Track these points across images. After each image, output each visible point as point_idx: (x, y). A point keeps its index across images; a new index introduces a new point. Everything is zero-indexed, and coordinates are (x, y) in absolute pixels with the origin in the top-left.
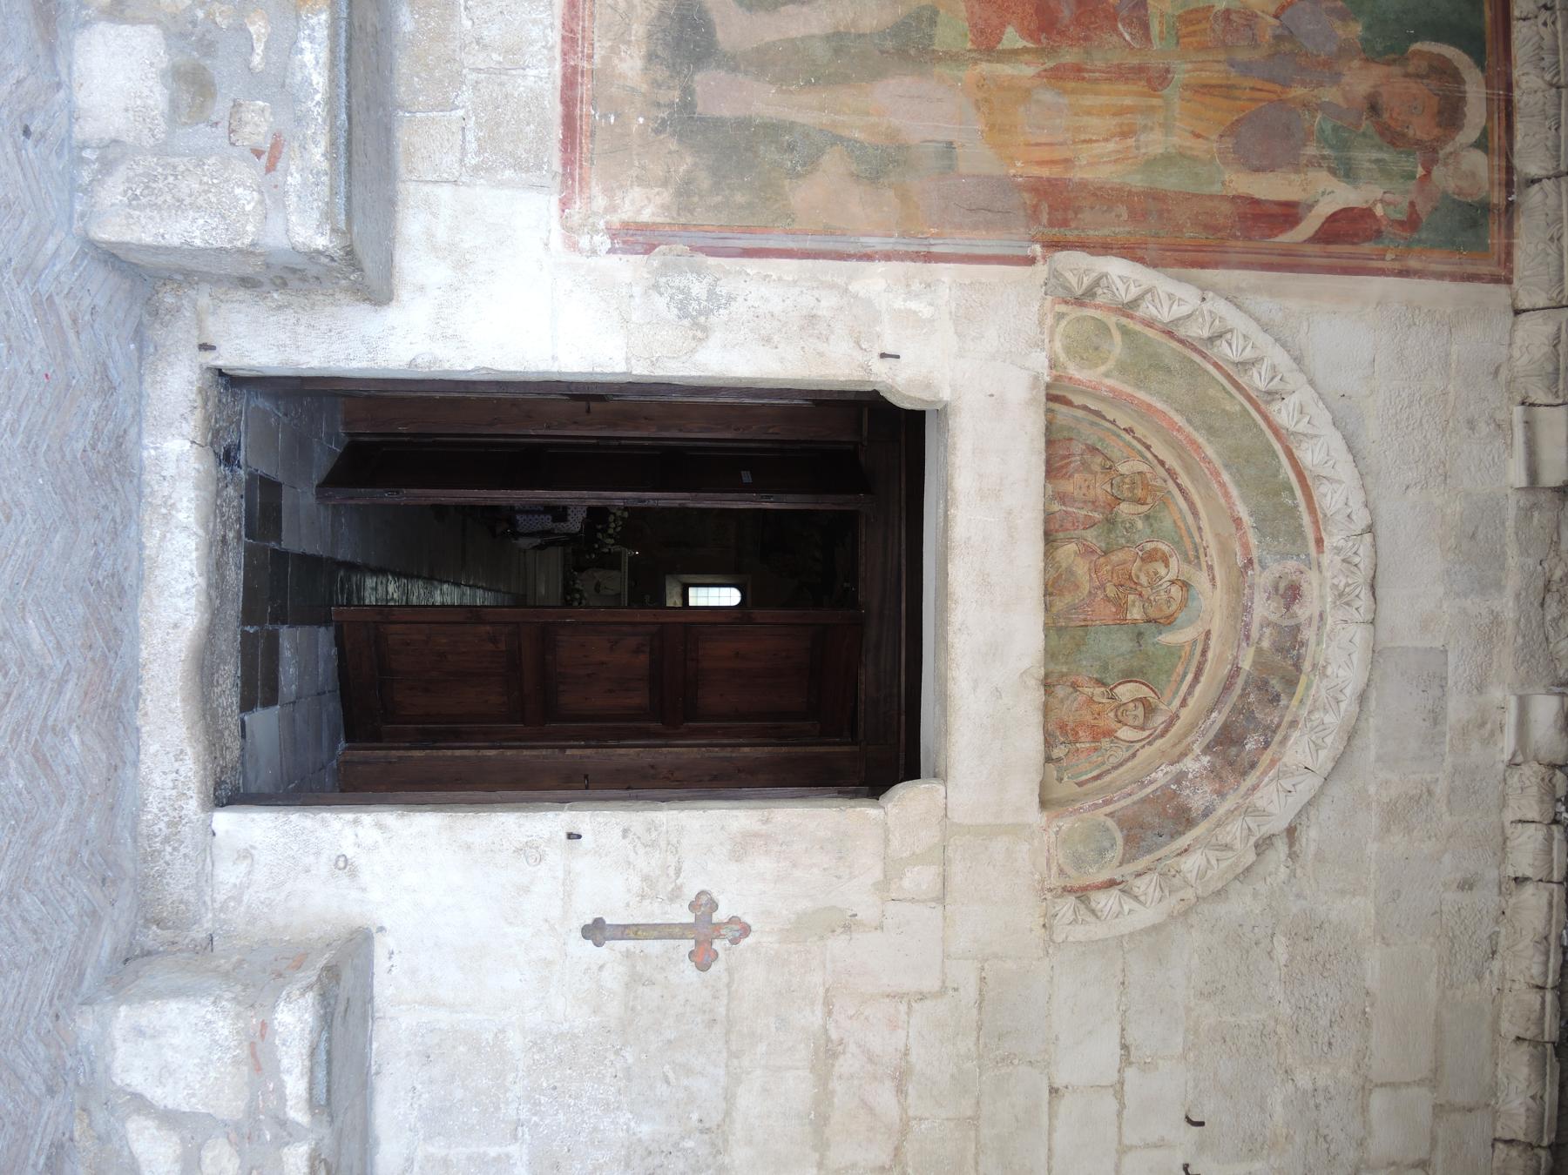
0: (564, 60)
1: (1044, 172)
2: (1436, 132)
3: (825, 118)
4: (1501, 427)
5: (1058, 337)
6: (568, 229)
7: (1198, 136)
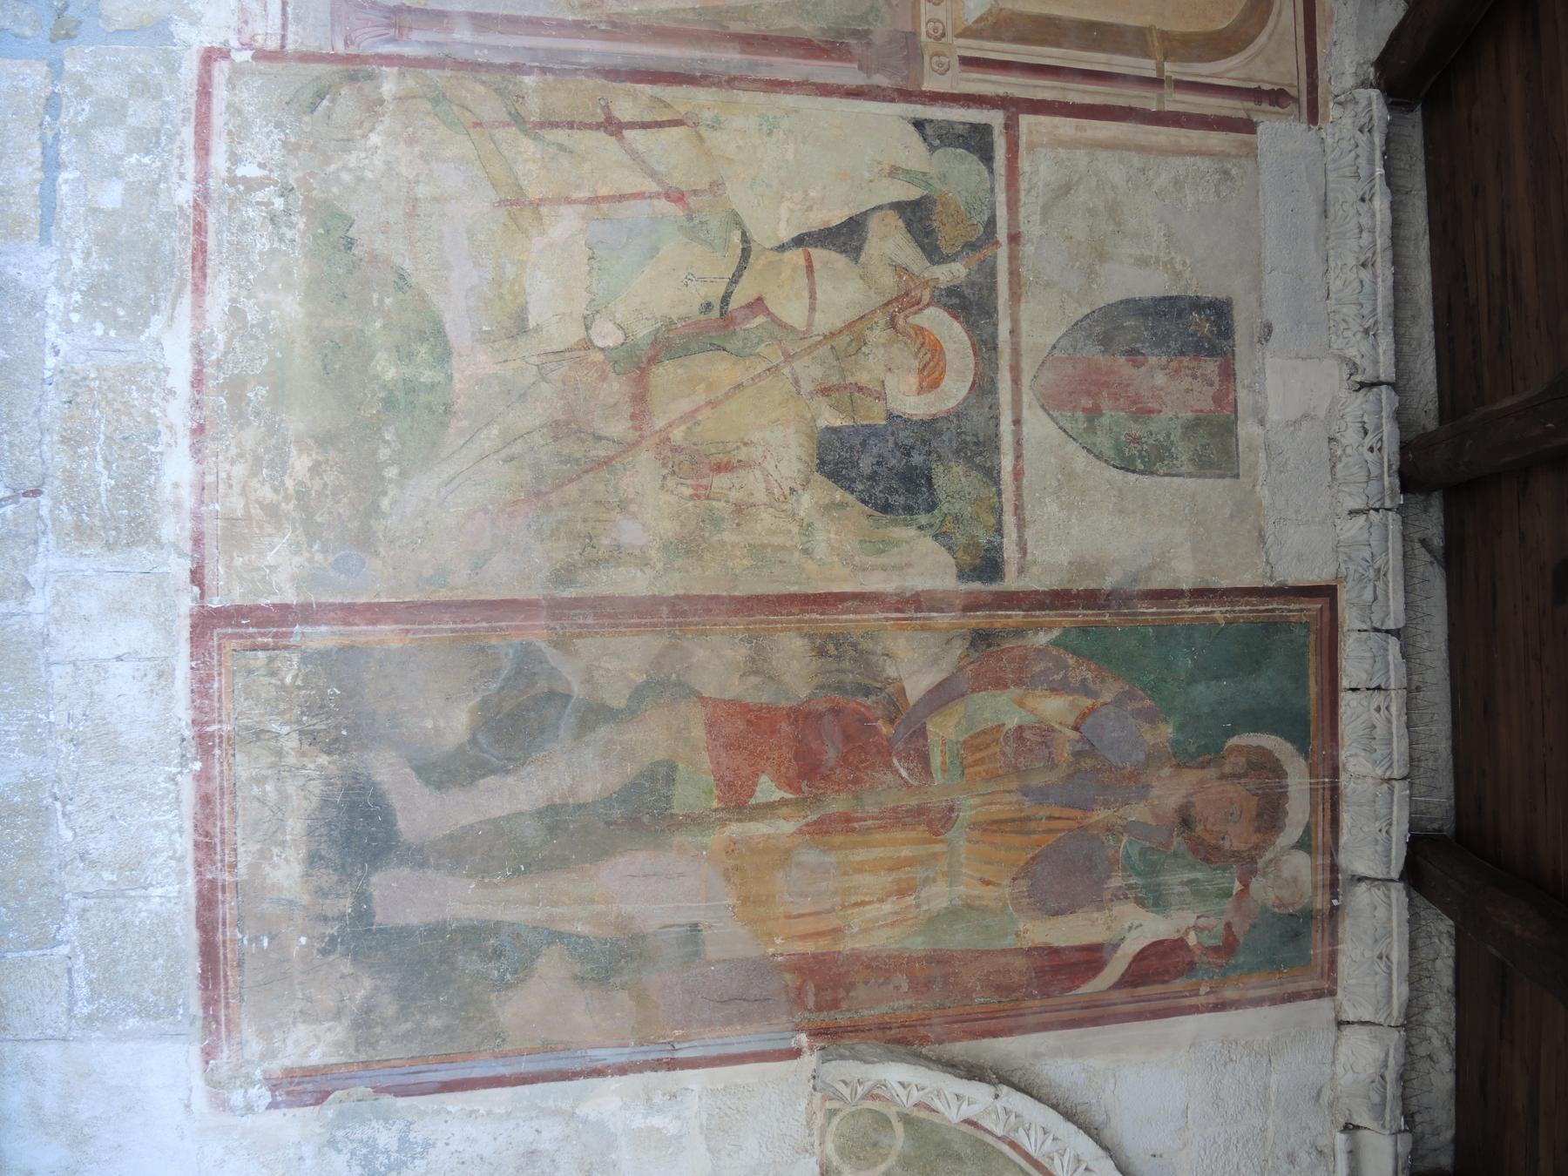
0: (199, 873)
1: (809, 947)
2: (1254, 838)
3: (539, 913)
5: (829, 1138)
6: (213, 1083)
7: (987, 883)
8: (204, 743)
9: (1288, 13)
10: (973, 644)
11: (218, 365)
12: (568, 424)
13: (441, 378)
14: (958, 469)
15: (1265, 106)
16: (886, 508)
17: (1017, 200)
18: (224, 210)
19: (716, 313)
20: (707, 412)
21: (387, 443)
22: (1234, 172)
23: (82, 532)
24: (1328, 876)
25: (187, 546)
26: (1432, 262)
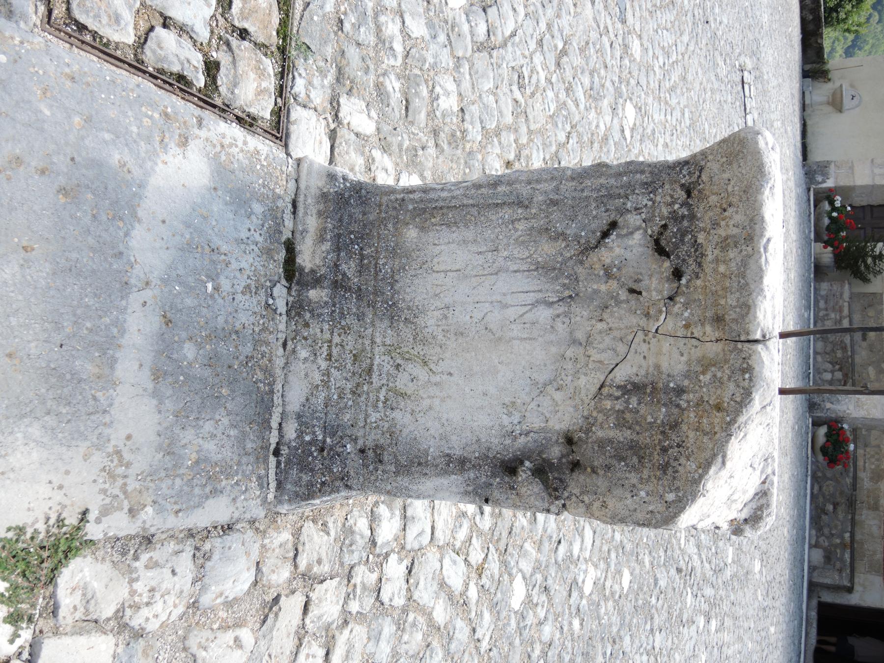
23: (869, 509)
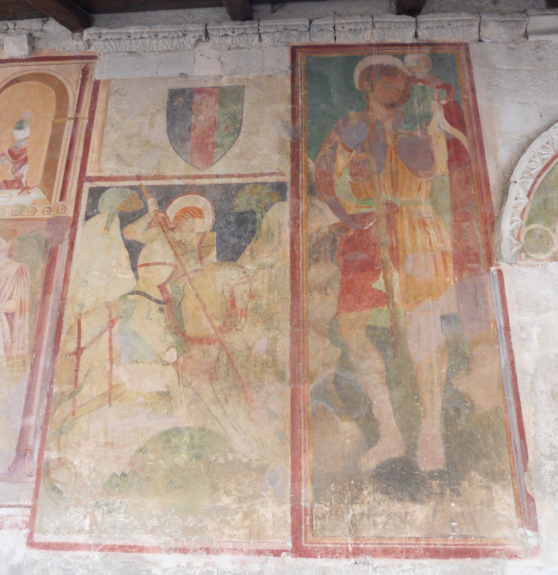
0: (421, 557)
1: (451, 266)
2: (399, 77)
3: (437, 390)
4: (538, 46)
7: (420, 188)
8: (357, 552)
9: (50, 67)
10: (314, 195)
11: (177, 540)
12: (211, 373)
13: (187, 432)
14: (237, 201)
15: (89, 76)
16: (253, 232)
17: (122, 177)
18: (105, 536)
19: (164, 306)
20: (208, 310)
21: (217, 458)
22: (115, 89)
24: (415, 47)
25: (262, 558)
26: (156, 10)
